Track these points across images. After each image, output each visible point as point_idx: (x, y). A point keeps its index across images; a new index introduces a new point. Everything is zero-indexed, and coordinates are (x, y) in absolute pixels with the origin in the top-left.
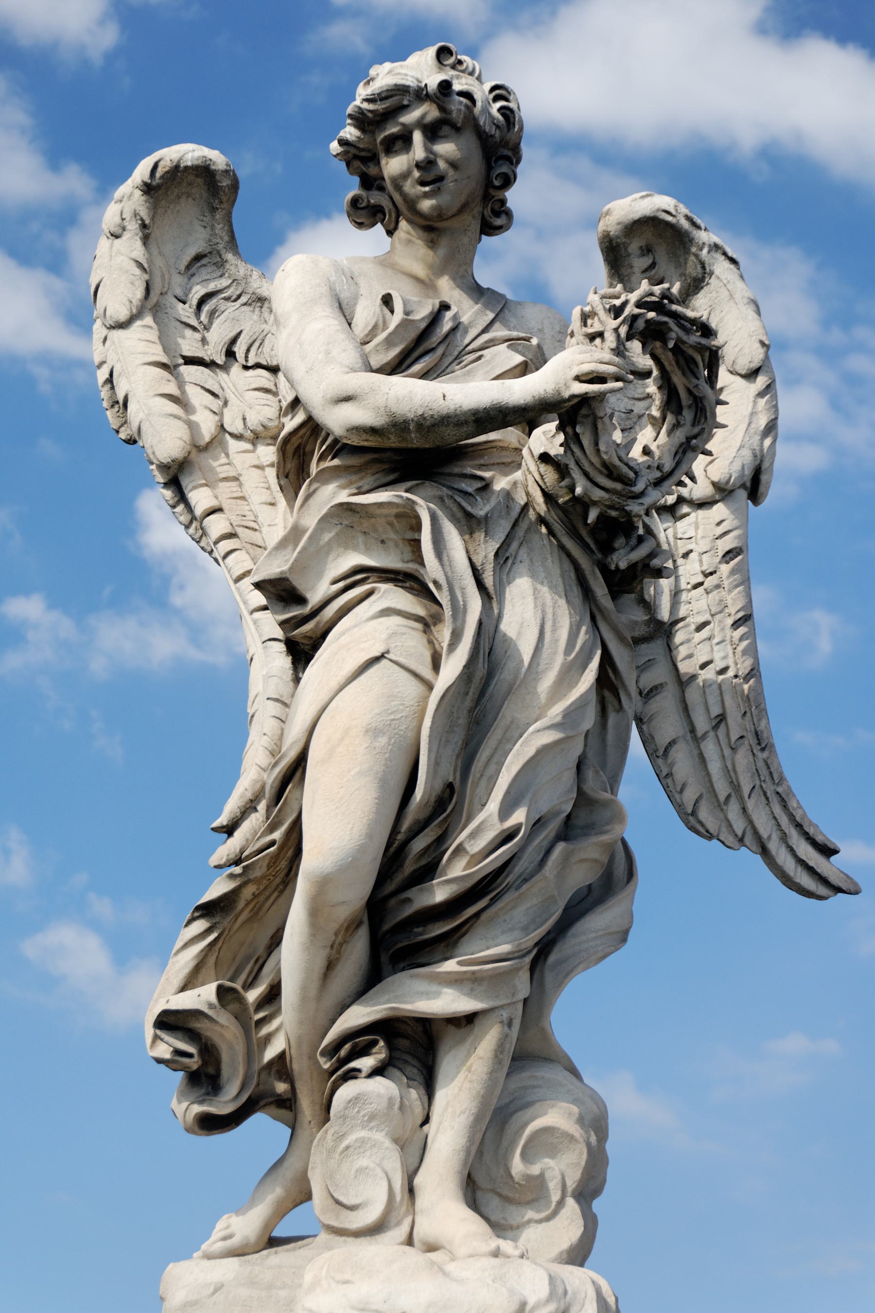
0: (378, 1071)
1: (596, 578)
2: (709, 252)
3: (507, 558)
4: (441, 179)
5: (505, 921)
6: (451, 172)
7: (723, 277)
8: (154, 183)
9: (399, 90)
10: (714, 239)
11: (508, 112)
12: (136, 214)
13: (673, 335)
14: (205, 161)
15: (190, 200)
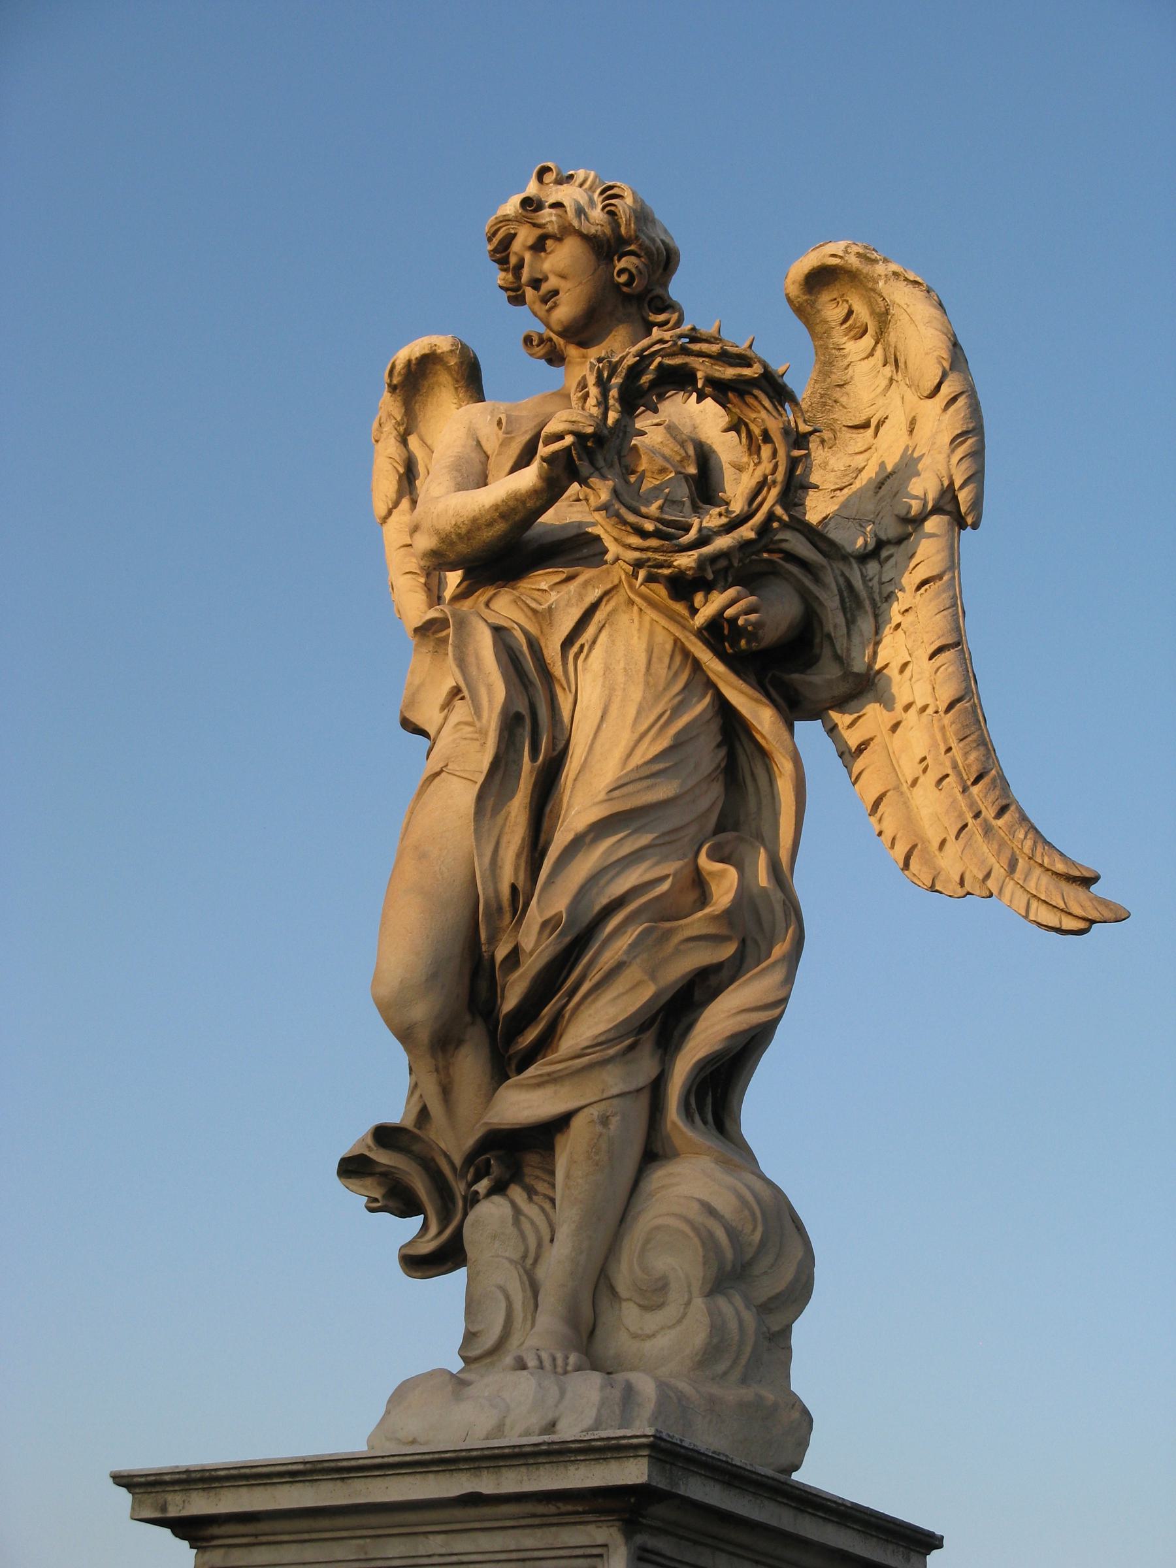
0: (498, 1189)
1: (694, 644)
2: (886, 282)
3: (582, 646)
4: (556, 293)
5: (590, 1016)
6: (563, 285)
7: (902, 303)
8: (395, 382)
9: (501, 222)
10: (894, 267)
11: (612, 208)
12: (390, 415)
13: (700, 375)
14: (431, 347)
15: (443, 389)
